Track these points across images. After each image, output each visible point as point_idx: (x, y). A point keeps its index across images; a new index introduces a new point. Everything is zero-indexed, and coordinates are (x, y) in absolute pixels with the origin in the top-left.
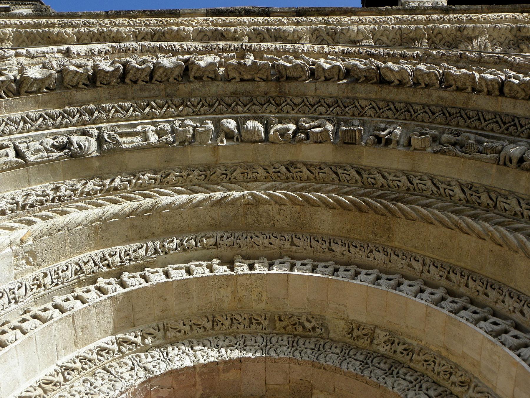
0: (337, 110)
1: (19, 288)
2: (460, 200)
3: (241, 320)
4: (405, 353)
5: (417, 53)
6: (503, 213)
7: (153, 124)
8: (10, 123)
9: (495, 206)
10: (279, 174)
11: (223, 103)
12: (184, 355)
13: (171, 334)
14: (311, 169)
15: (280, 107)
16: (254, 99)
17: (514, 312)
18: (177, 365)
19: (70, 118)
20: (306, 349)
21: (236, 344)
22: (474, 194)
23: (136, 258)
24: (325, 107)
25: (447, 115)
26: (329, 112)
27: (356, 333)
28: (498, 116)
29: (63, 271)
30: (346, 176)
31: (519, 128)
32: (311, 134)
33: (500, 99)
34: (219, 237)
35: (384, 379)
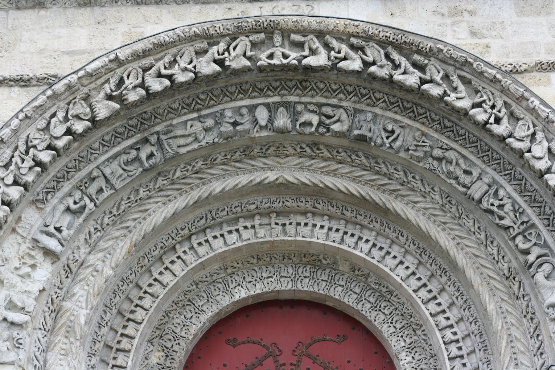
0: (355, 98)
1: (131, 274)
2: (438, 203)
3: (277, 257)
4: (387, 293)
5: (431, 47)
6: (463, 225)
7: (199, 119)
8: (93, 152)
9: (460, 218)
10: (304, 153)
11: (256, 89)
12: (240, 288)
13: (229, 271)
14: (331, 150)
15: (305, 92)
16: (283, 83)
17: (454, 295)
18: (237, 297)
19: (134, 130)
20: (322, 280)
21: (274, 274)
22: (448, 203)
23: (200, 227)
24: (345, 95)
25: (443, 127)
26: (348, 99)
27: (356, 272)
28: (479, 142)
29: (154, 251)
30: (358, 162)
31: (490, 160)
32: (331, 130)
33: (483, 132)
34: (259, 203)
35: (370, 312)
